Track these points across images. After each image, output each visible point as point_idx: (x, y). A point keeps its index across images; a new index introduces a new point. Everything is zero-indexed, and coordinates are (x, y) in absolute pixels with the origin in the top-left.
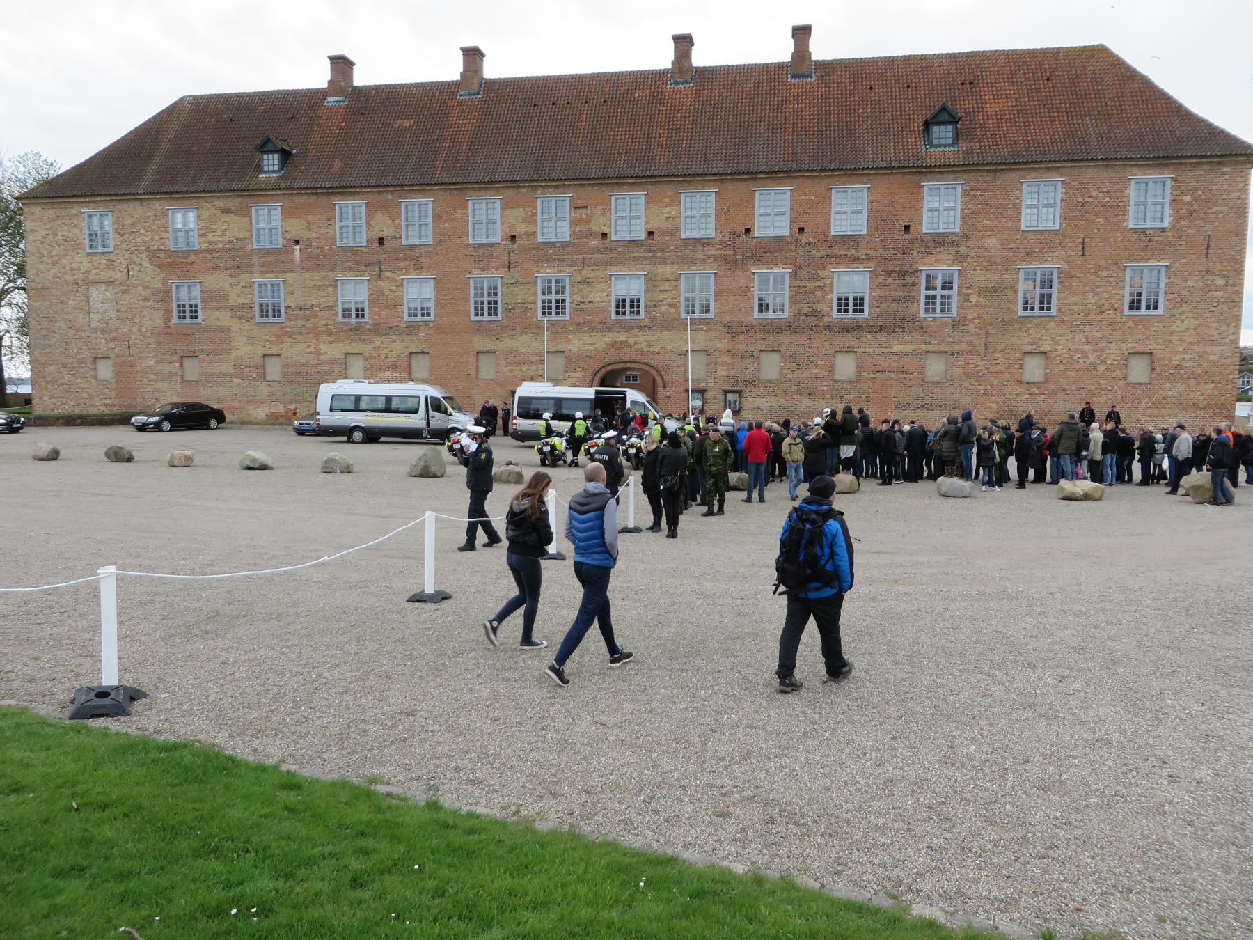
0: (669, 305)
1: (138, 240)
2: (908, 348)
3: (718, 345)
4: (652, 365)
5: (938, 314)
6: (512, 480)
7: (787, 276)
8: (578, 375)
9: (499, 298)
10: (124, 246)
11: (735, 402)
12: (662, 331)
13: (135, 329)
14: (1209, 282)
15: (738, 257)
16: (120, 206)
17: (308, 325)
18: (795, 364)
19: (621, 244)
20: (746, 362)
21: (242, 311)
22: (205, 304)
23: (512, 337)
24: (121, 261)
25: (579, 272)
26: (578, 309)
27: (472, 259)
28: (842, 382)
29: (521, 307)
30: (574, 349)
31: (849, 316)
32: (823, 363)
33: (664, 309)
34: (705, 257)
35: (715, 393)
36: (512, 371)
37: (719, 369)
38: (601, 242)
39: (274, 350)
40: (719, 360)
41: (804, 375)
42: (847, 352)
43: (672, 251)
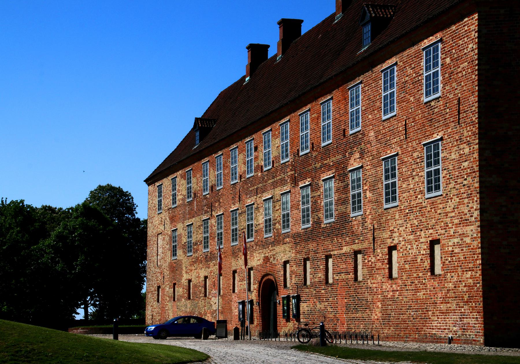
14: (462, 153)
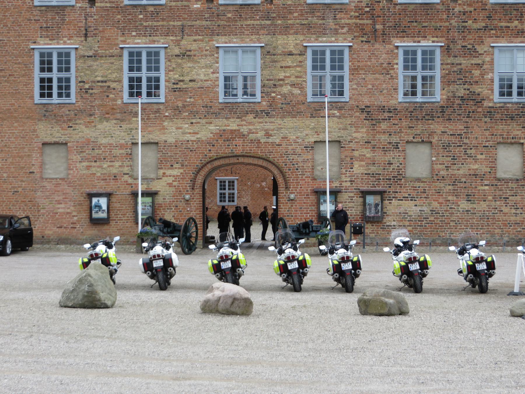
0: (293, 85)
3: (354, 135)
4: (271, 160)
6: (238, 310)
7: (438, 52)
8: (175, 172)
9: (73, 74)
11: (377, 205)
12: (283, 117)
15: (377, 27)
18: (449, 159)
19: (231, 8)
20: (389, 156)
23: (88, 124)
25: (177, 43)
27: (38, 25)
28: (507, 181)
29: (101, 87)
30: (171, 140)
31: (514, 100)
32: (483, 157)
33: (286, 89)
34: (337, 27)
35: (352, 195)
36: (88, 167)
37: (356, 165)
38: (206, 5)
40: (356, 154)
41: (461, 172)
42: (512, 144)
43: (296, 18)
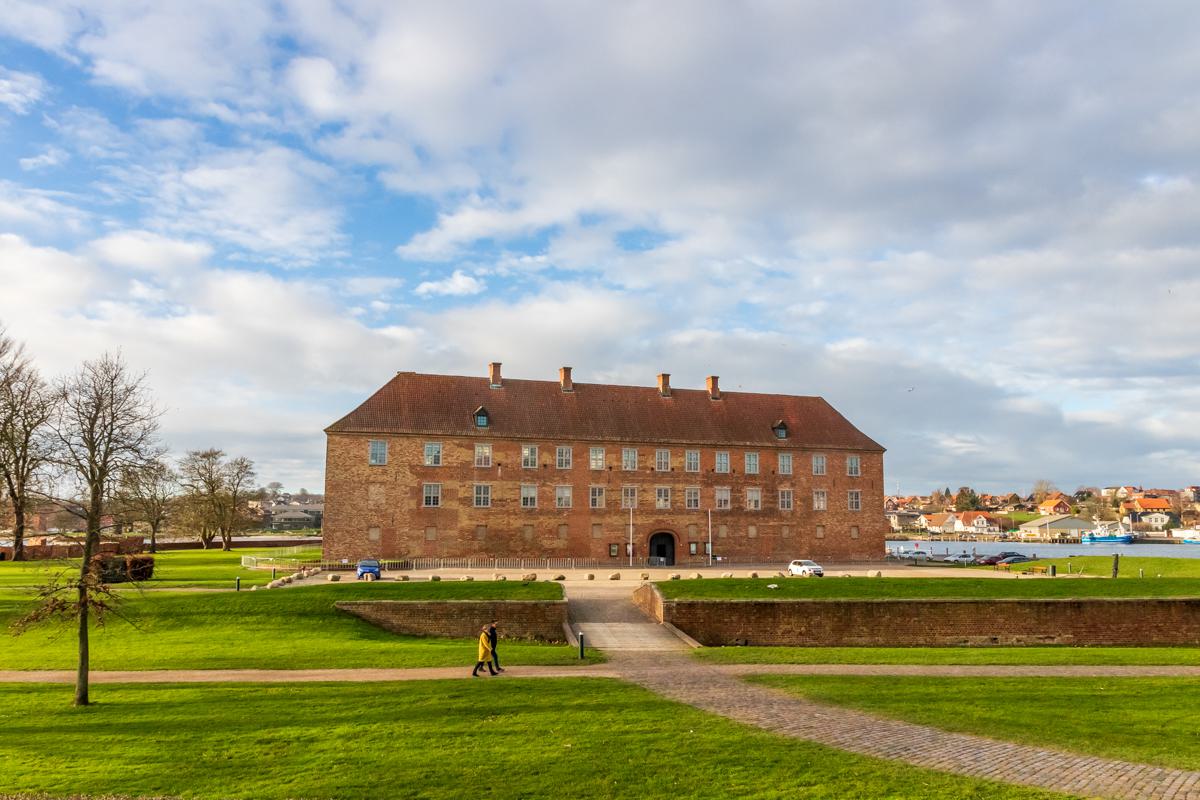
1: (404, 459)
2: (776, 523)
5: (786, 508)
8: (642, 535)
10: (395, 462)
13: (397, 510)
16: (393, 439)
17: (504, 509)
21: (466, 501)
22: (444, 497)
24: (392, 470)
26: (641, 503)
39: (484, 523)
